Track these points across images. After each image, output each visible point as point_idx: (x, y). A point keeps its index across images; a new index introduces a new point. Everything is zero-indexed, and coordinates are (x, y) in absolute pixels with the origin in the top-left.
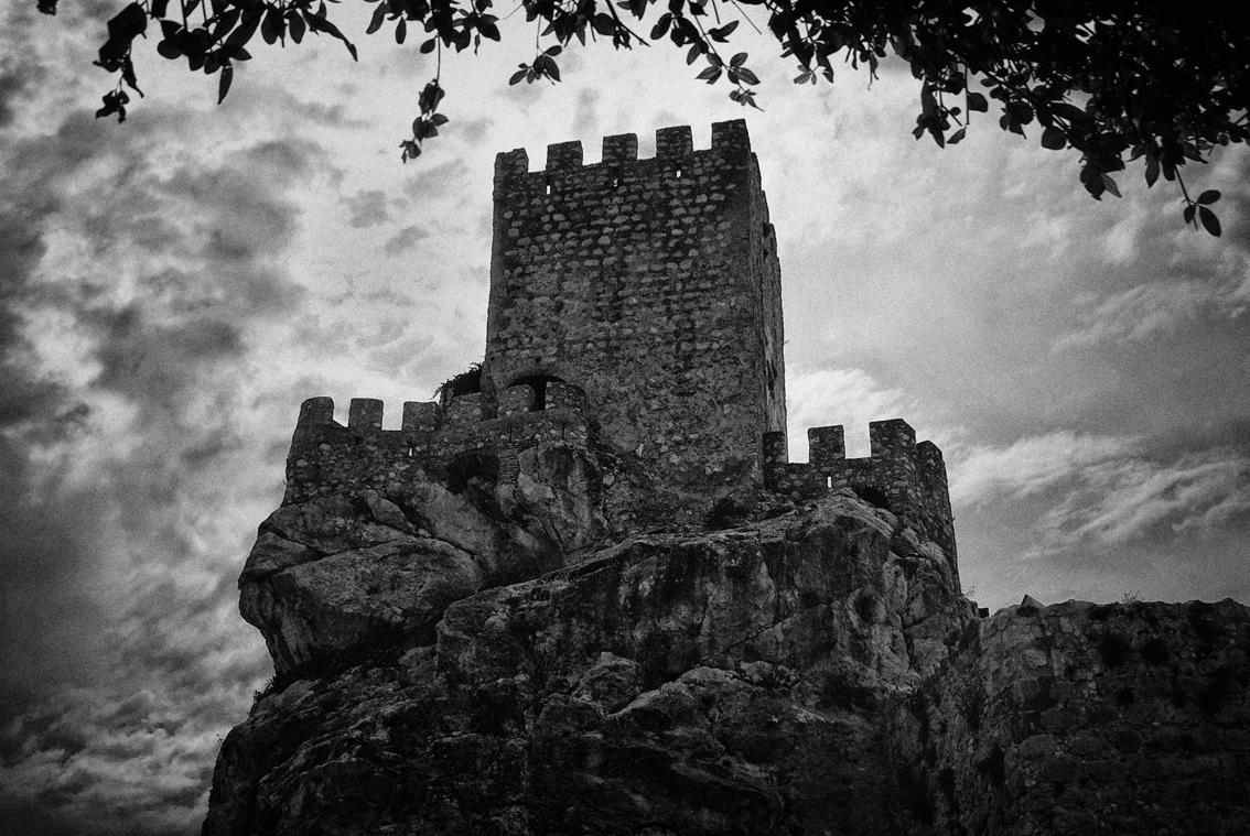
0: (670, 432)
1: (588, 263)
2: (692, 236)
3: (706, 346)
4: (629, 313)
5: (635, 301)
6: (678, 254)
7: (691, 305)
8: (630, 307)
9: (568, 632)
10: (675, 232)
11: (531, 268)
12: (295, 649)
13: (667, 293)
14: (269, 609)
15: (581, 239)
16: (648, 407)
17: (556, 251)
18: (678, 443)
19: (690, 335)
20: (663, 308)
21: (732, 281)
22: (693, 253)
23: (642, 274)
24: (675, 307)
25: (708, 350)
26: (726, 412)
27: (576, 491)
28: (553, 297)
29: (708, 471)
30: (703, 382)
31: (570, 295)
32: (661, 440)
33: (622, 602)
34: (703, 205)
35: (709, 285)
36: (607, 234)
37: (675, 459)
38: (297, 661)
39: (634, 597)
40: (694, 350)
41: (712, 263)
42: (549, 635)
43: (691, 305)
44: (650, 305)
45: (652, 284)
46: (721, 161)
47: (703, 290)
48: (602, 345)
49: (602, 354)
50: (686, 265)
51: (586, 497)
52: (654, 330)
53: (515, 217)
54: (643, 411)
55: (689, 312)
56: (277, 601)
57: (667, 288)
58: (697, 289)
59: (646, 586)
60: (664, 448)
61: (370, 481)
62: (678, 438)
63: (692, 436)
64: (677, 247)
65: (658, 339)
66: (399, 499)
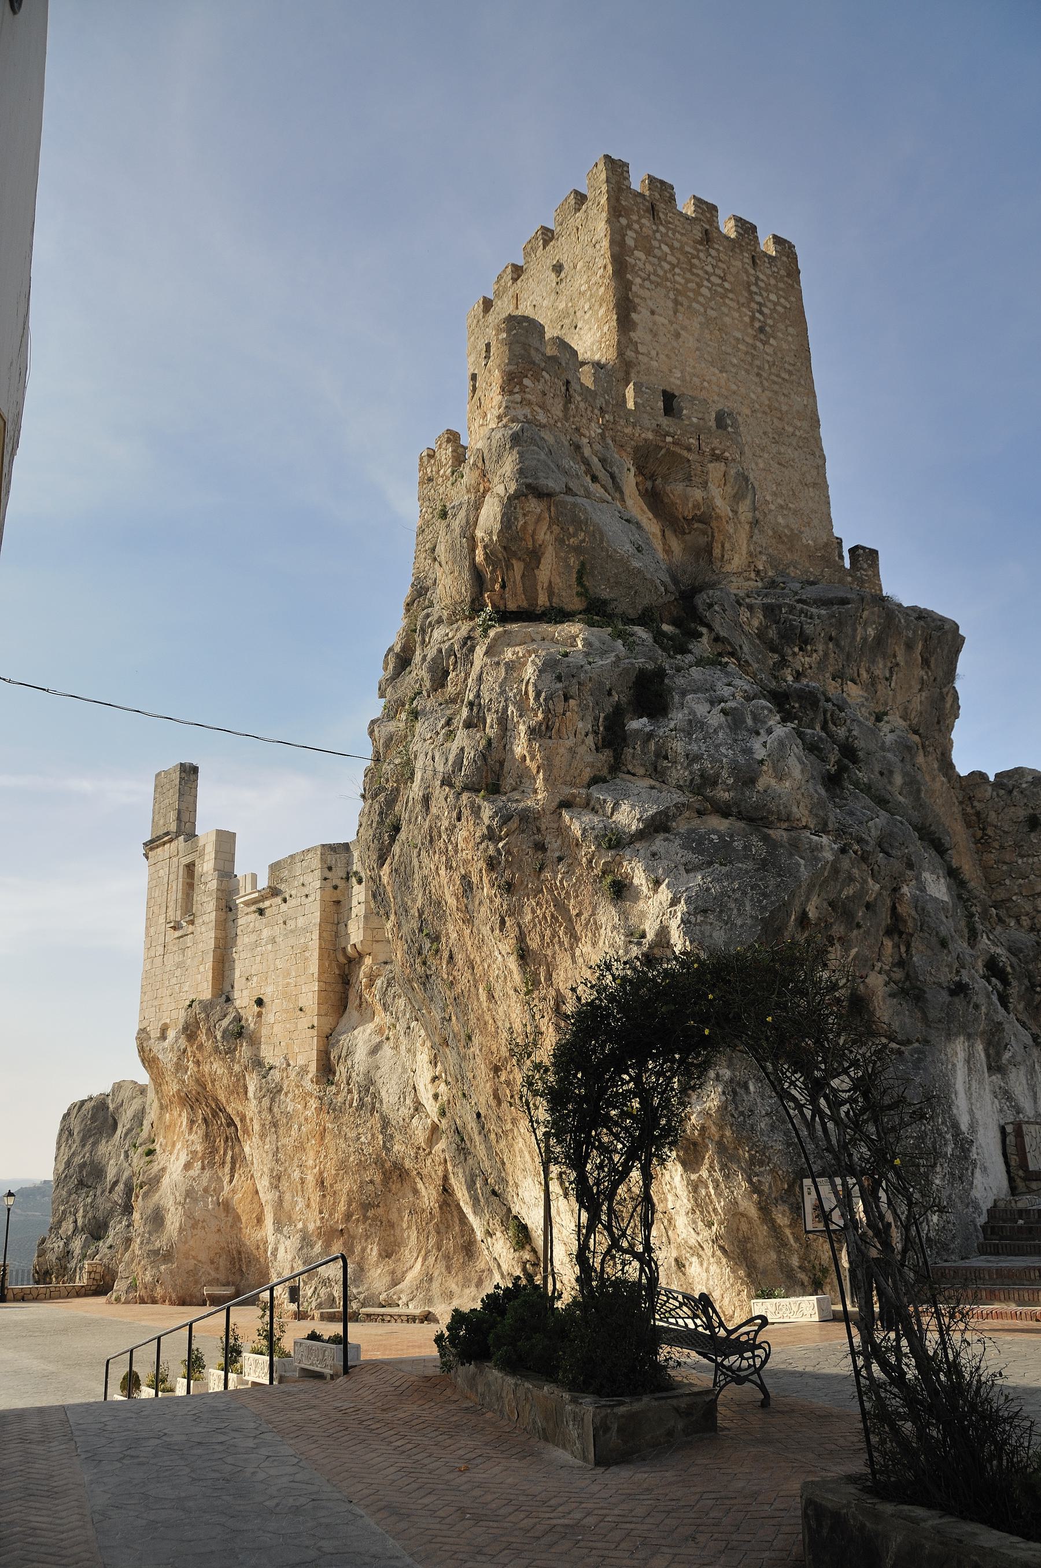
0: (775, 494)
1: (694, 305)
2: (771, 326)
3: (790, 429)
4: (734, 370)
5: (735, 361)
6: (762, 336)
7: (776, 387)
8: (734, 365)
9: (826, 655)
10: (757, 315)
11: (647, 284)
12: (546, 585)
13: (759, 368)
14: (542, 534)
15: (688, 281)
16: (757, 464)
17: (667, 280)
18: (781, 507)
19: (779, 415)
20: (757, 380)
21: (803, 382)
22: (772, 341)
23: (738, 339)
24: (766, 384)
25: (793, 434)
26: (812, 494)
27: (743, 518)
28: (671, 323)
29: (804, 541)
30: (793, 460)
31: (684, 328)
32: (768, 498)
33: (858, 639)
34: (775, 304)
35: (787, 377)
36: (707, 287)
37: (780, 520)
38: (542, 600)
39: (865, 639)
40: (783, 429)
41: (787, 359)
42: (816, 651)
43: (776, 387)
44: (747, 371)
45: (747, 353)
46: (783, 272)
47: (783, 379)
48: (716, 389)
49: (716, 398)
50: (769, 350)
51: (747, 527)
52: (753, 396)
53: (629, 226)
54: (753, 466)
55: (776, 393)
56: (550, 527)
57: (757, 362)
58: (778, 376)
59: (871, 632)
60: (772, 507)
61: (577, 429)
62: (780, 501)
63: (790, 505)
64: (761, 330)
65: (757, 406)
66: (603, 461)
